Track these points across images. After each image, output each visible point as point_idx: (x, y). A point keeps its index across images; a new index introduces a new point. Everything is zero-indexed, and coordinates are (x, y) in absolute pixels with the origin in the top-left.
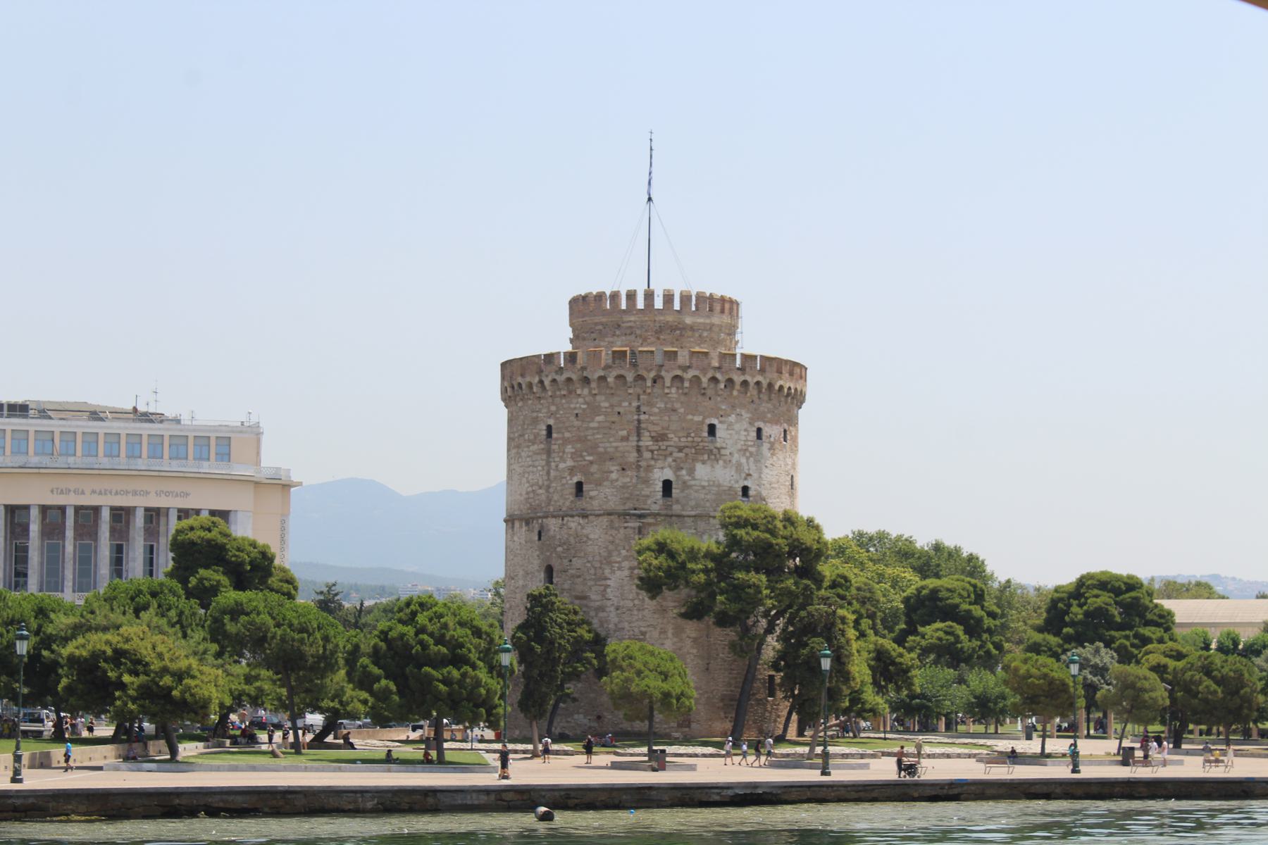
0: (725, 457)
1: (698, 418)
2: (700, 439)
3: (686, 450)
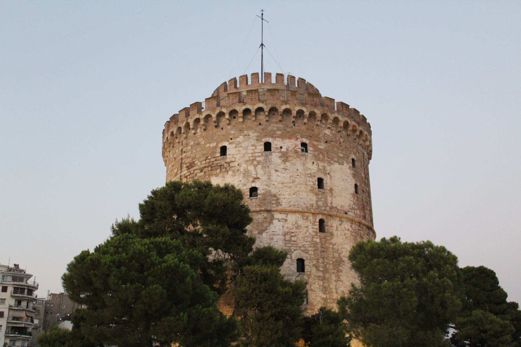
0: (233, 168)
1: (212, 145)
2: (215, 159)
3: (206, 170)
